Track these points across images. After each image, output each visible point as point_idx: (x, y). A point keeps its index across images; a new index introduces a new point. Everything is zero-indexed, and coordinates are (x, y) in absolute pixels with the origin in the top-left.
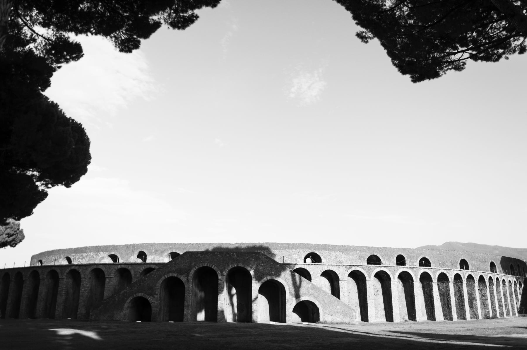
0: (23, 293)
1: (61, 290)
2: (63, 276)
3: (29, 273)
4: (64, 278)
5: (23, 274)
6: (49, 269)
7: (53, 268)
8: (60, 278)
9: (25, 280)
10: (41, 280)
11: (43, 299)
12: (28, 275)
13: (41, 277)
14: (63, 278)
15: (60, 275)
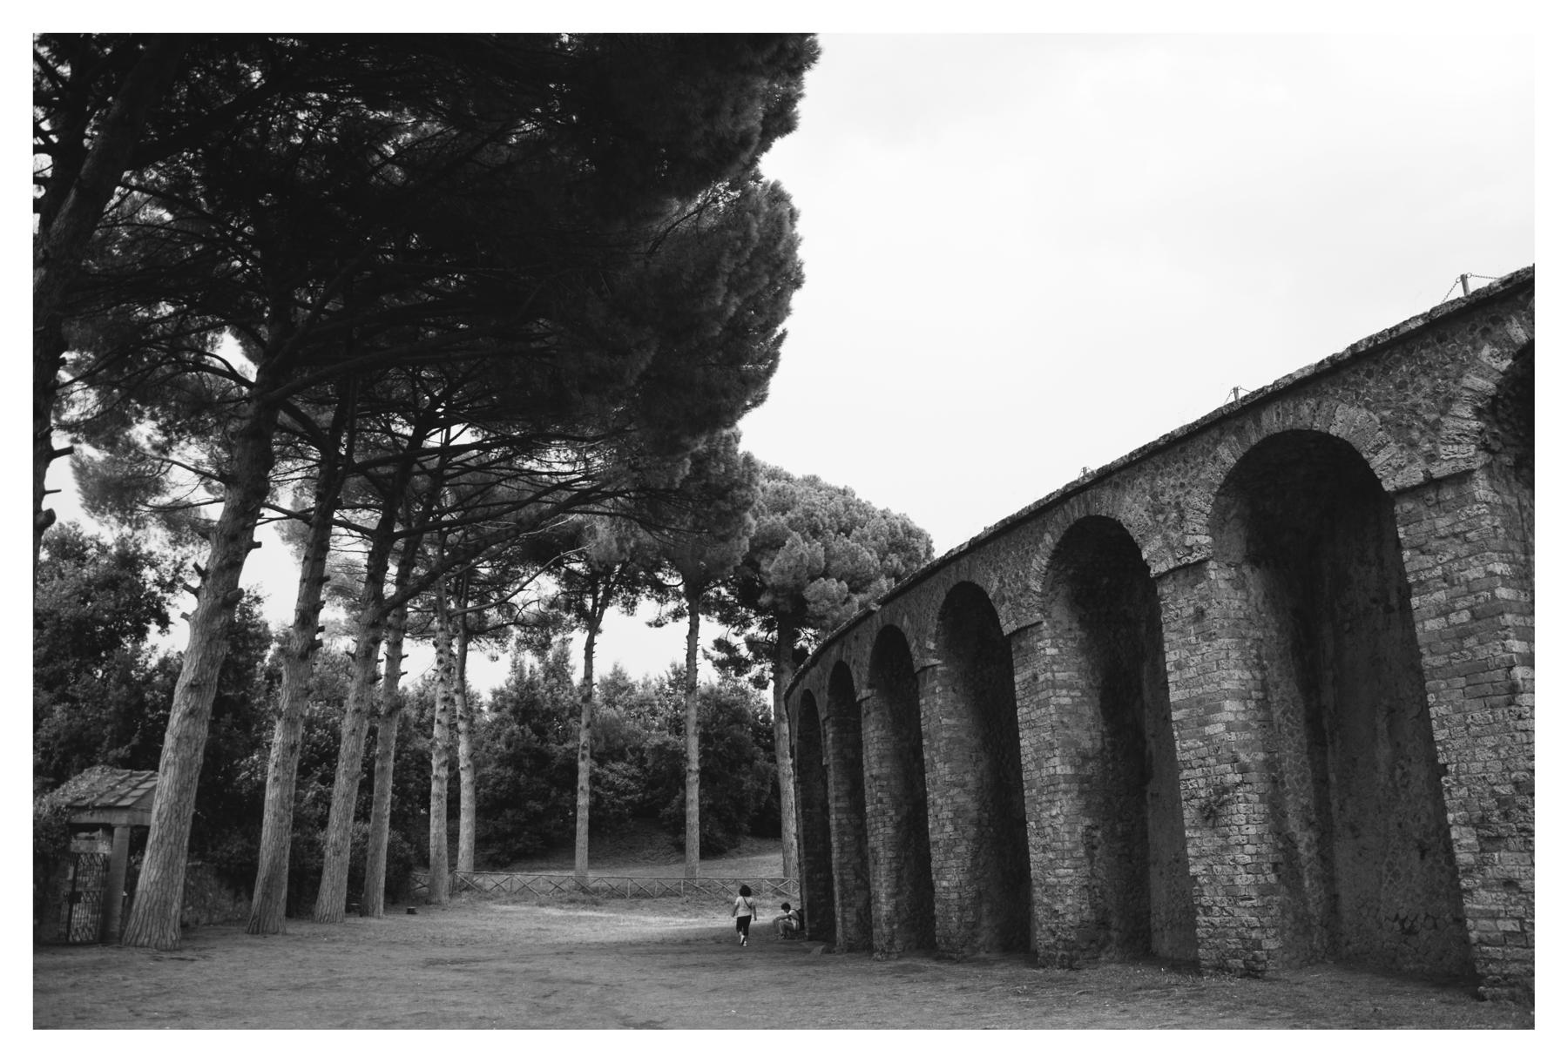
0: (1026, 741)
1: (1465, 616)
2: (1431, 458)
3: (1039, 562)
4: (1461, 478)
5: (993, 588)
6: (1228, 454)
7: (1272, 421)
8: (1402, 492)
9: (1021, 632)
10: (1165, 590)
11: (1244, 770)
12: (1036, 586)
13: (1157, 556)
14: (1438, 471)
15: (1378, 462)
